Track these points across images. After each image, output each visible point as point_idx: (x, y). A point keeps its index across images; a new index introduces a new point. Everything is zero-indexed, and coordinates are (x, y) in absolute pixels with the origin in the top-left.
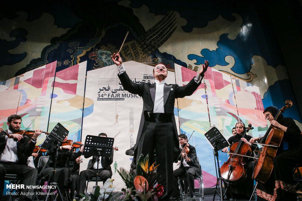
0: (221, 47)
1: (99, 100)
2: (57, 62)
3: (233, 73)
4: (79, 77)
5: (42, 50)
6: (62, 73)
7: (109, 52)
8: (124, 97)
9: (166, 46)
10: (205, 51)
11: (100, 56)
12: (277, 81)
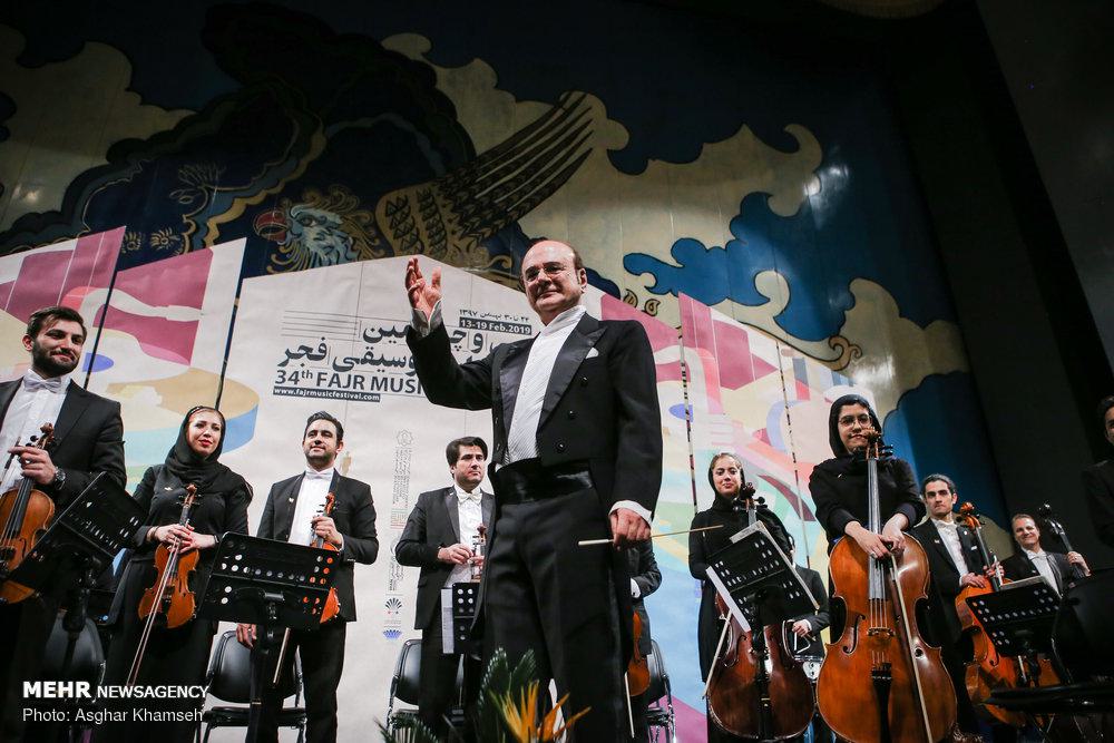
0: (743, 237)
1: (280, 394)
2: (127, 233)
3: (781, 333)
4: (208, 299)
5: (68, 181)
6: (143, 274)
7: (333, 218)
8: (379, 389)
9: (548, 215)
10: (684, 248)
11: (296, 228)
12: (930, 376)
